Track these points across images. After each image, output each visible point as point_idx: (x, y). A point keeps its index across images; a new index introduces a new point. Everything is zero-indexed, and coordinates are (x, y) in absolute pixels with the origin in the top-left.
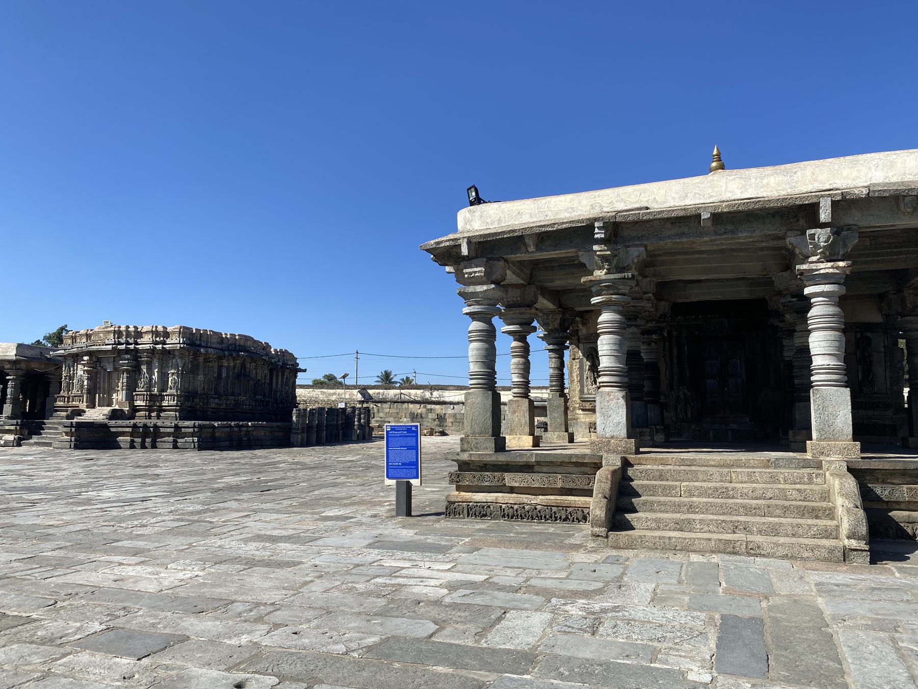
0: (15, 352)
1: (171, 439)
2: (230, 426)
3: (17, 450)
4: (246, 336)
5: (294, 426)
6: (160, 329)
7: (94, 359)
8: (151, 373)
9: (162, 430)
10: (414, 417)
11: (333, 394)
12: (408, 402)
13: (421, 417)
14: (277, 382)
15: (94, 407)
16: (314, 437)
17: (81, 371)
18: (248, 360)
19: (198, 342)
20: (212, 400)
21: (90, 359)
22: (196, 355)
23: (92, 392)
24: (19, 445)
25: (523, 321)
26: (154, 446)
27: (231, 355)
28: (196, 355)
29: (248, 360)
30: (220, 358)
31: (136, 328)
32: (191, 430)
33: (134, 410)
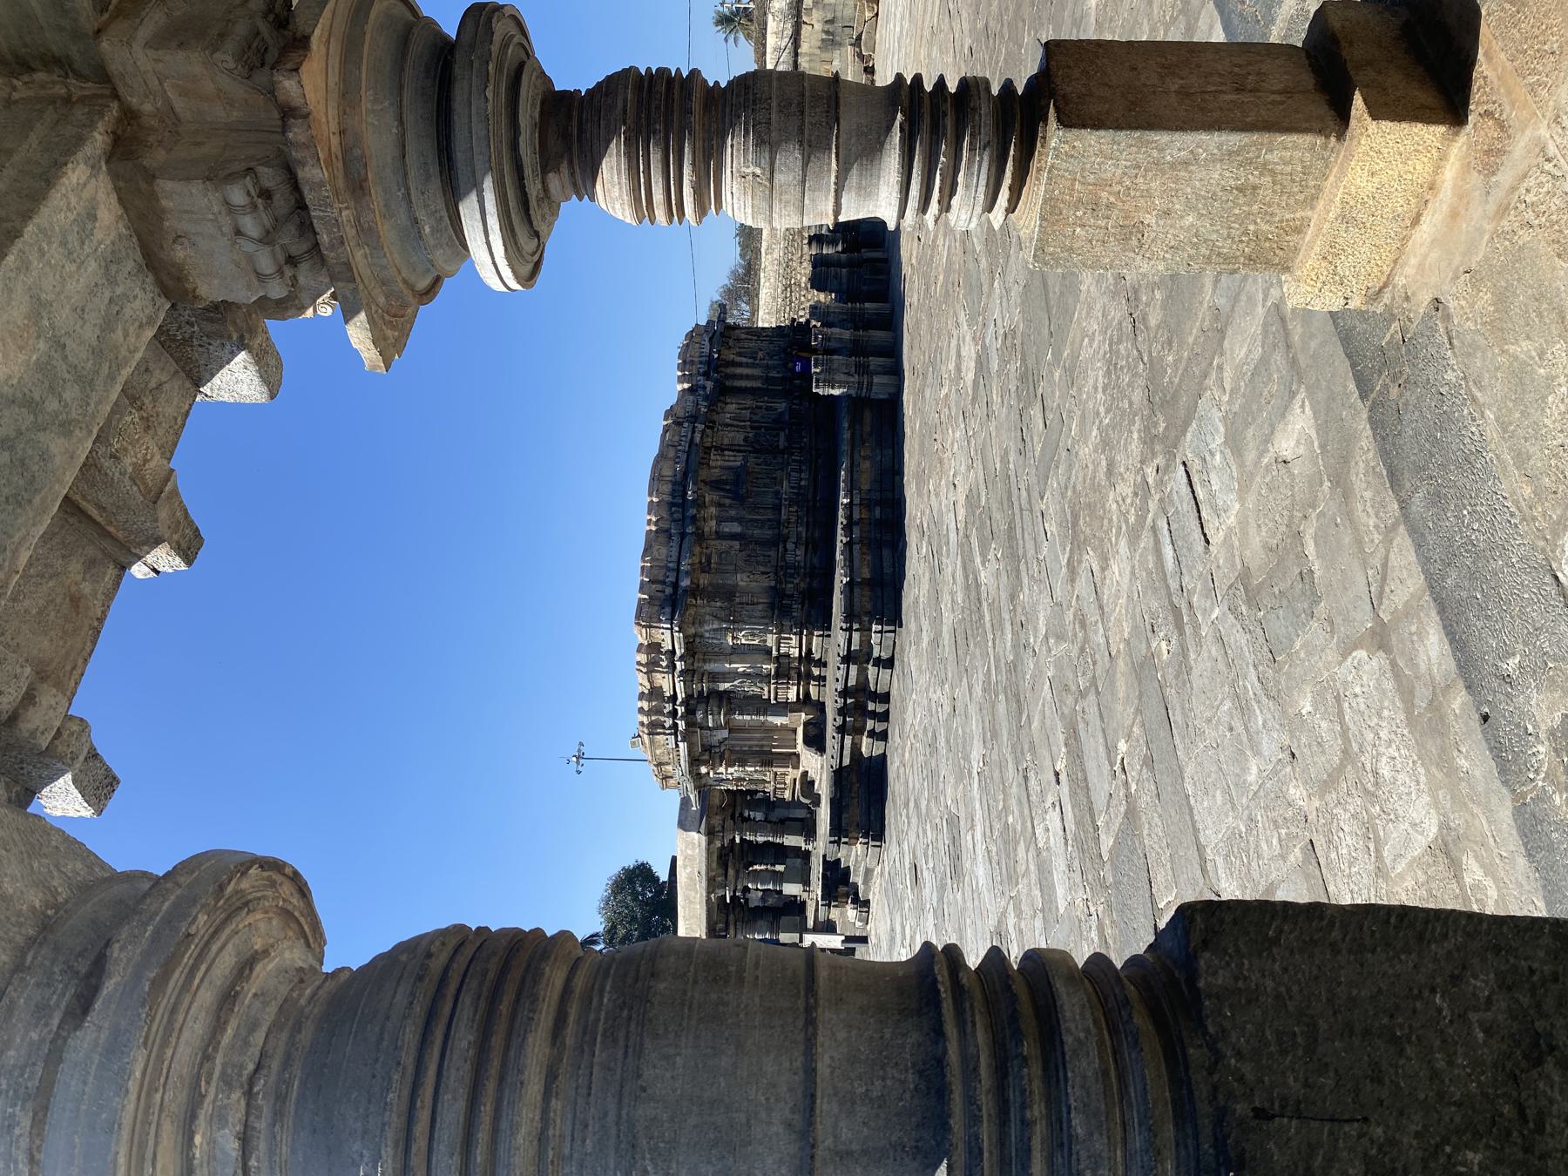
0: (694, 835)
1: (872, 671)
2: (849, 545)
3: (875, 896)
4: (653, 479)
5: (853, 392)
6: (643, 658)
7: (706, 757)
8: (735, 675)
9: (852, 682)
10: (830, 42)
12: (796, 54)
13: (831, 22)
14: (747, 377)
15: (797, 756)
16: (878, 335)
17: (729, 774)
18: (704, 474)
19: (669, 590)
20: (789, 558)
21: (705, 763)
22: (695, 591)
23: (767, 759)
24: (866, 903)
25: (420, 150)
26: (885, 698)
27: (694, 519)
28: (695, 591)
29: (704, 474)
30: (700, 537)
31: (642, 696)
32: (856, 636)
33: (805, 701)
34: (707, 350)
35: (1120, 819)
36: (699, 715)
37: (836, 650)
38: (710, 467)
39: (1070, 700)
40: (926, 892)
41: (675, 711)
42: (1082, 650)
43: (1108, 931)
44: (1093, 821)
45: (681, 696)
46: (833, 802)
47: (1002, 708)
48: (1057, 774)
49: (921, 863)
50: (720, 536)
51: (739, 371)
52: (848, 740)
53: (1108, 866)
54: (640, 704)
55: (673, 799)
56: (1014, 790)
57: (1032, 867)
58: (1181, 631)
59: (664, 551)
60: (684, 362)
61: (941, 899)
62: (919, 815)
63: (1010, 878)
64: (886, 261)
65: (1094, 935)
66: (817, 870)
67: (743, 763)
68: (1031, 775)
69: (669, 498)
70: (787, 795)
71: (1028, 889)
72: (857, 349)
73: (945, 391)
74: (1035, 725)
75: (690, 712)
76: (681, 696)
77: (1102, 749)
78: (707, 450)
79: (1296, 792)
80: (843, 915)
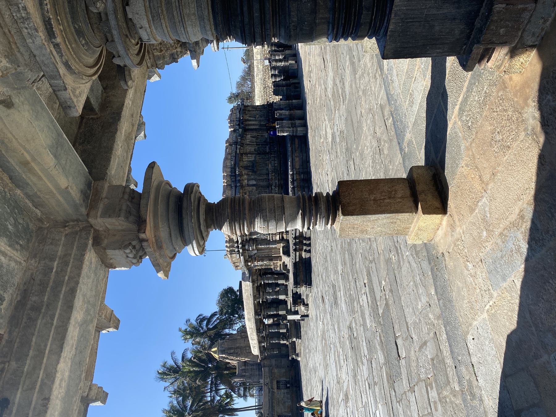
0: (248, 283)
2: (293, 188)
3: (310, 302)
4: (224, 167)
5: (291, 134)
11: (258, 68)
14: (254, 125)
16: (298, 112)
18: (241, 164)
21: (250, 262)
23: (271, 259)
24: (307, 305)
26: (309, 239)
27: (239, 180)
30: (242, 186)
31: (226, 242)
34: (238, 116)
35: (384, 305)
36: (247, 247)
37: (292, 236)
38: (243, 161)
39: (367, 262)
40: (327, 306)
41: (238, 246)
42: (370, 248)
43: (382, 338)
44: (376, 303)
45: (240, 241)
46: (294, 274)
47: (347, 256)
48: (365, 284)
49: (324, 296)
50: (248, 185)
51: (250, 123)
52: (298, 253)
53: (381, 318)
54: (226, 244)
55: (240, 272)
56: (352, 284)
57: (359, 311)
58: (398, 256)
59: (230, 192)
60: (231, 121)
61: (331, 310)
62: (323, 281)
63: (352, 311)
64: (299, 83)
65: (378, 338)
66: (290, 294)
67: (263, 261)
68: (357, 281)
69: (230, 174)
70: (278, 269)
71: (358, 315)
72: (291, 118)
73: (322, 140)
74: (357, 266)
75: (243, 246)
76: (240, 241)
77: (377, 282)
78: (242, 154)
79: (431, 316)
80: (301, 309)
